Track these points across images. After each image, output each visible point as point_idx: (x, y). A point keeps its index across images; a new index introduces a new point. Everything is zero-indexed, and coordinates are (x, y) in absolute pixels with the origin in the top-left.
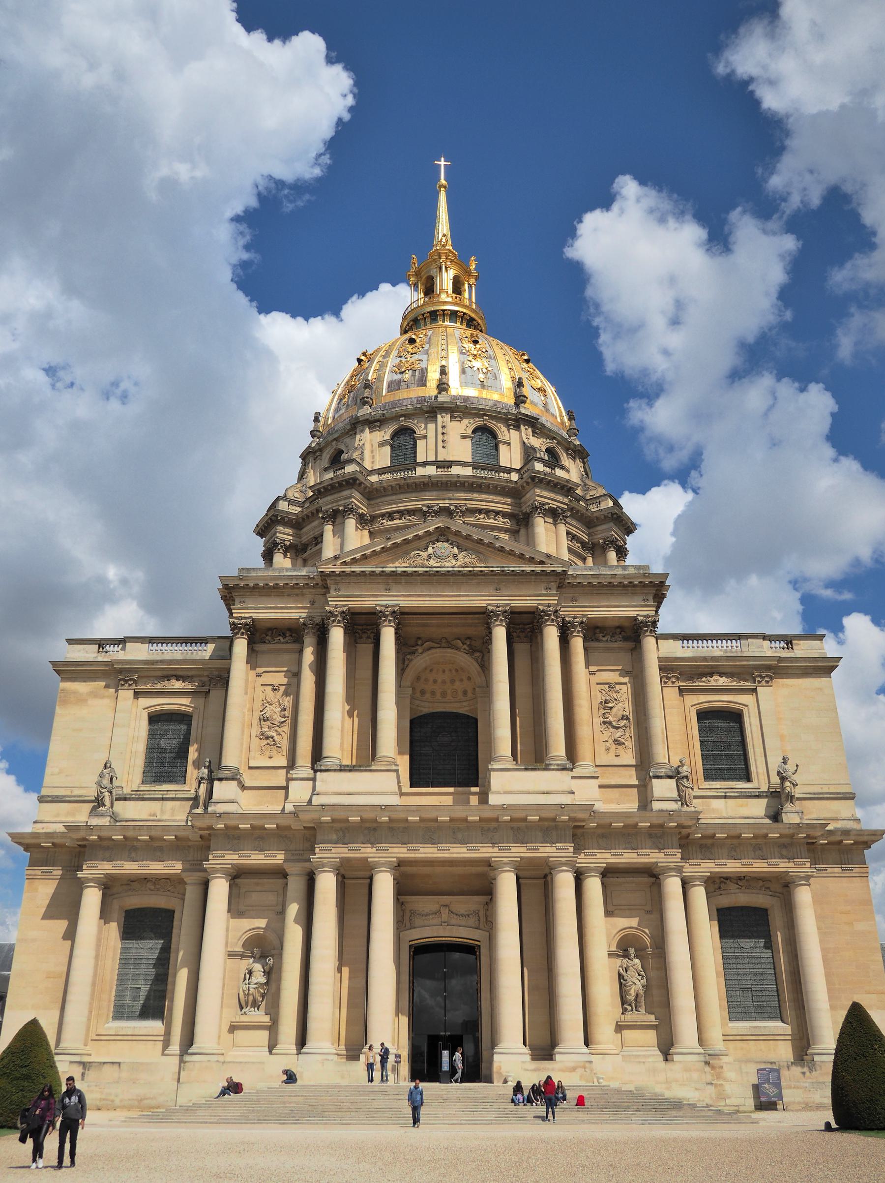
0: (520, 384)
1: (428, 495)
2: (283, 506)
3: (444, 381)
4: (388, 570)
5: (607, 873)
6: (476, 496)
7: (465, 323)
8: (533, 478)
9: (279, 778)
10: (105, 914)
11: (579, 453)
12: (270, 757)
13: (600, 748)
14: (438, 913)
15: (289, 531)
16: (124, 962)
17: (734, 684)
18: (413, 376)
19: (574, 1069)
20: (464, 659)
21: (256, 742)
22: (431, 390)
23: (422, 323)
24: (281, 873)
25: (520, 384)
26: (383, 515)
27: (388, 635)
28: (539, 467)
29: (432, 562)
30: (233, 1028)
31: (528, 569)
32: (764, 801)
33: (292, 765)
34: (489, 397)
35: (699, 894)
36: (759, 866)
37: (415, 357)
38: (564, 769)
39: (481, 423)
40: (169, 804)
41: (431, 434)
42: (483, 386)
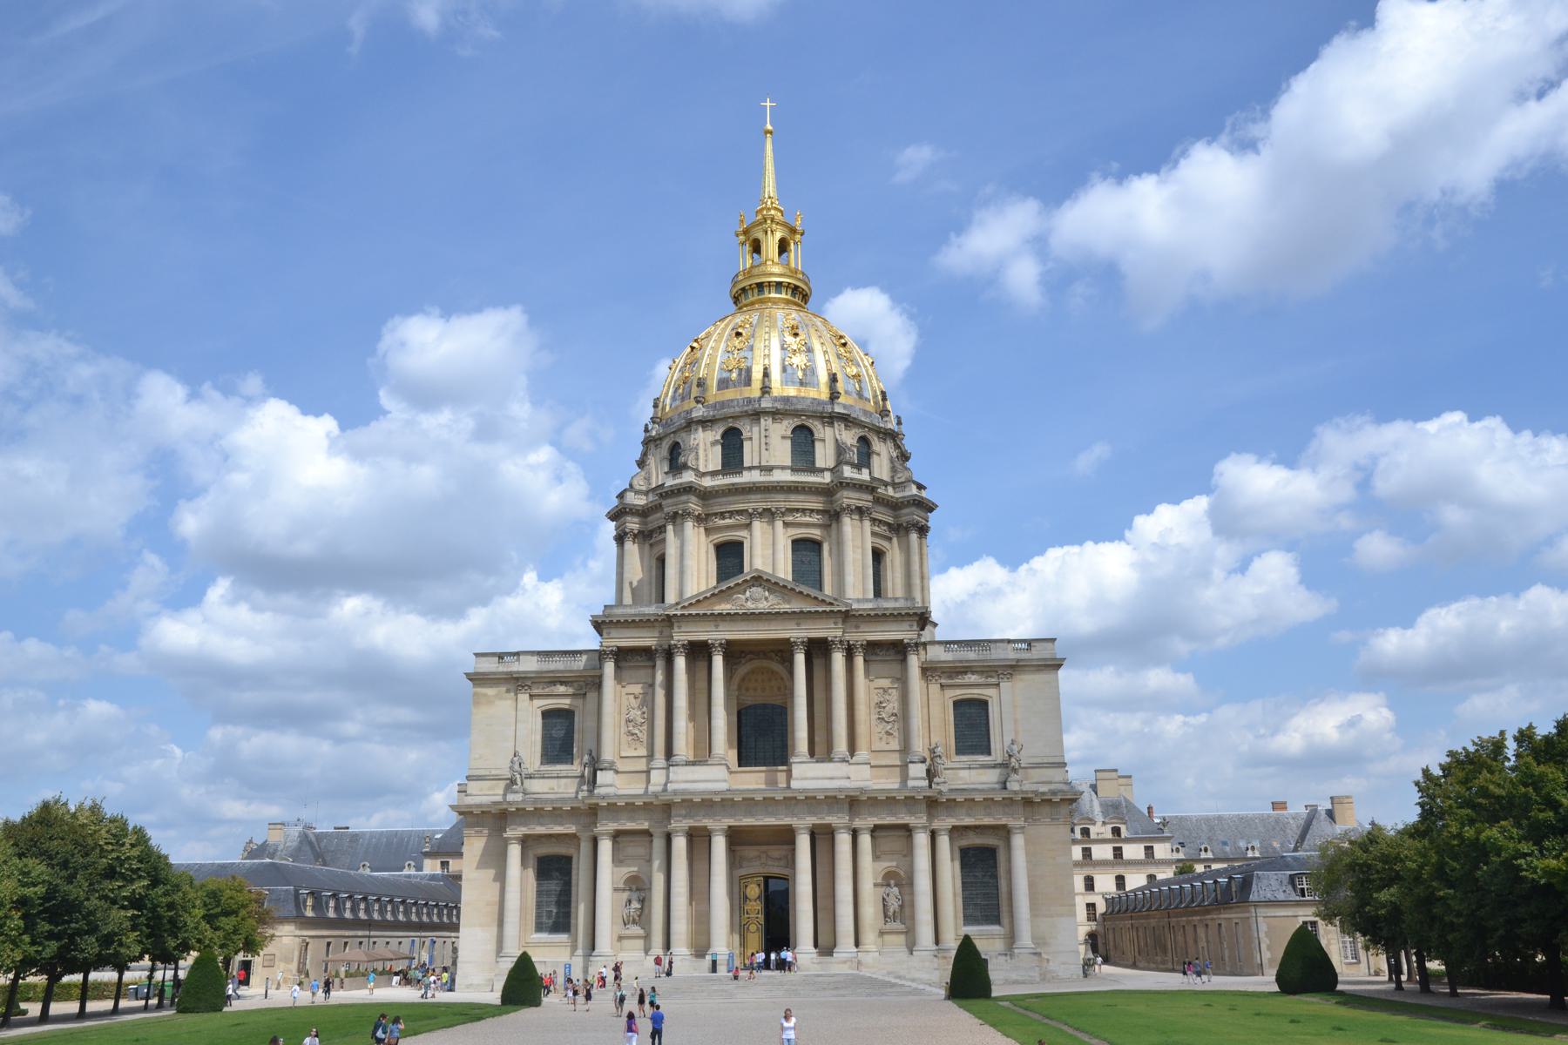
2: (632, 499)
5: (875, 830)
6: (793, 497)
9: (641, 765)
10: (524, 864)
11: (892, 436)
13: (875, 738)
15: (636, 520)
16: (539, 893)
17: (982, 680)
21: (624, 738)
22: (755, 391)
24: (647, 833)
25: (833, 379)
27: (718, 661)
28: (848, 472)
30: (620, 938)
32: (997, 771)
33: (651, 756)
35: (944, 842)
37: (742, 354)
38: (844, 760)
41: (755, 436)
42: (802, 383)
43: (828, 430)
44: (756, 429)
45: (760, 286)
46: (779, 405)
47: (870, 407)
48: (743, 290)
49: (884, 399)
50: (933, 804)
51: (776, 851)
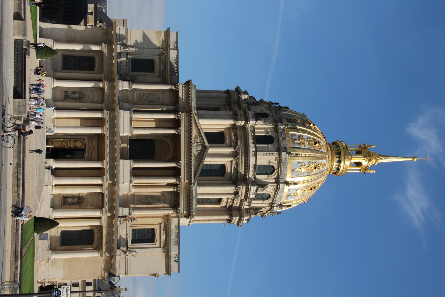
0: (295, 184)
1: (243, 148)
3: (293, 155)
4: (192, 131)
5: (102, 194)
7: (337, 166)
8: (249, 185)
12: (138, 98)
14: (92, 147)
18: (297, 144)
19: (49, 180)
20: (170, 156)
23: (337, 149)
25: (295, 184)
26: (236, 132)
27: (172, 132)
29: (195, 144)
31: (192, 173)
34: (288, 172)
36: (104, 240)
39: (275, 168)
40: (125, 68)
43: (273, 181)
44: (274, 149)
45: (339, 154)
46: (283, 160)
47: (284, 200)
48: (338, 146)
49: (288, 206)
50: (112, 218)
51: (94, 154)
